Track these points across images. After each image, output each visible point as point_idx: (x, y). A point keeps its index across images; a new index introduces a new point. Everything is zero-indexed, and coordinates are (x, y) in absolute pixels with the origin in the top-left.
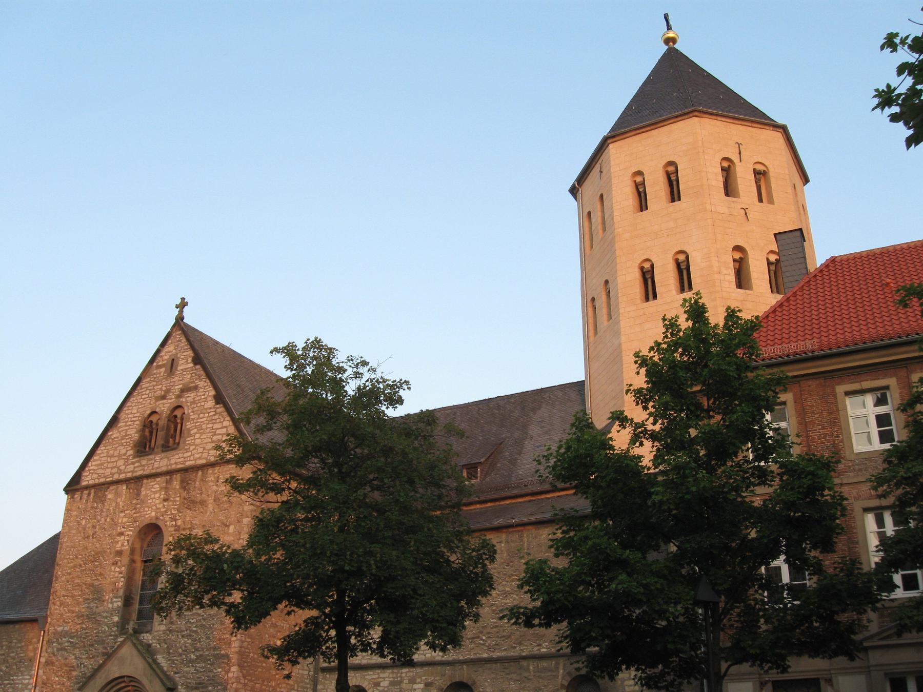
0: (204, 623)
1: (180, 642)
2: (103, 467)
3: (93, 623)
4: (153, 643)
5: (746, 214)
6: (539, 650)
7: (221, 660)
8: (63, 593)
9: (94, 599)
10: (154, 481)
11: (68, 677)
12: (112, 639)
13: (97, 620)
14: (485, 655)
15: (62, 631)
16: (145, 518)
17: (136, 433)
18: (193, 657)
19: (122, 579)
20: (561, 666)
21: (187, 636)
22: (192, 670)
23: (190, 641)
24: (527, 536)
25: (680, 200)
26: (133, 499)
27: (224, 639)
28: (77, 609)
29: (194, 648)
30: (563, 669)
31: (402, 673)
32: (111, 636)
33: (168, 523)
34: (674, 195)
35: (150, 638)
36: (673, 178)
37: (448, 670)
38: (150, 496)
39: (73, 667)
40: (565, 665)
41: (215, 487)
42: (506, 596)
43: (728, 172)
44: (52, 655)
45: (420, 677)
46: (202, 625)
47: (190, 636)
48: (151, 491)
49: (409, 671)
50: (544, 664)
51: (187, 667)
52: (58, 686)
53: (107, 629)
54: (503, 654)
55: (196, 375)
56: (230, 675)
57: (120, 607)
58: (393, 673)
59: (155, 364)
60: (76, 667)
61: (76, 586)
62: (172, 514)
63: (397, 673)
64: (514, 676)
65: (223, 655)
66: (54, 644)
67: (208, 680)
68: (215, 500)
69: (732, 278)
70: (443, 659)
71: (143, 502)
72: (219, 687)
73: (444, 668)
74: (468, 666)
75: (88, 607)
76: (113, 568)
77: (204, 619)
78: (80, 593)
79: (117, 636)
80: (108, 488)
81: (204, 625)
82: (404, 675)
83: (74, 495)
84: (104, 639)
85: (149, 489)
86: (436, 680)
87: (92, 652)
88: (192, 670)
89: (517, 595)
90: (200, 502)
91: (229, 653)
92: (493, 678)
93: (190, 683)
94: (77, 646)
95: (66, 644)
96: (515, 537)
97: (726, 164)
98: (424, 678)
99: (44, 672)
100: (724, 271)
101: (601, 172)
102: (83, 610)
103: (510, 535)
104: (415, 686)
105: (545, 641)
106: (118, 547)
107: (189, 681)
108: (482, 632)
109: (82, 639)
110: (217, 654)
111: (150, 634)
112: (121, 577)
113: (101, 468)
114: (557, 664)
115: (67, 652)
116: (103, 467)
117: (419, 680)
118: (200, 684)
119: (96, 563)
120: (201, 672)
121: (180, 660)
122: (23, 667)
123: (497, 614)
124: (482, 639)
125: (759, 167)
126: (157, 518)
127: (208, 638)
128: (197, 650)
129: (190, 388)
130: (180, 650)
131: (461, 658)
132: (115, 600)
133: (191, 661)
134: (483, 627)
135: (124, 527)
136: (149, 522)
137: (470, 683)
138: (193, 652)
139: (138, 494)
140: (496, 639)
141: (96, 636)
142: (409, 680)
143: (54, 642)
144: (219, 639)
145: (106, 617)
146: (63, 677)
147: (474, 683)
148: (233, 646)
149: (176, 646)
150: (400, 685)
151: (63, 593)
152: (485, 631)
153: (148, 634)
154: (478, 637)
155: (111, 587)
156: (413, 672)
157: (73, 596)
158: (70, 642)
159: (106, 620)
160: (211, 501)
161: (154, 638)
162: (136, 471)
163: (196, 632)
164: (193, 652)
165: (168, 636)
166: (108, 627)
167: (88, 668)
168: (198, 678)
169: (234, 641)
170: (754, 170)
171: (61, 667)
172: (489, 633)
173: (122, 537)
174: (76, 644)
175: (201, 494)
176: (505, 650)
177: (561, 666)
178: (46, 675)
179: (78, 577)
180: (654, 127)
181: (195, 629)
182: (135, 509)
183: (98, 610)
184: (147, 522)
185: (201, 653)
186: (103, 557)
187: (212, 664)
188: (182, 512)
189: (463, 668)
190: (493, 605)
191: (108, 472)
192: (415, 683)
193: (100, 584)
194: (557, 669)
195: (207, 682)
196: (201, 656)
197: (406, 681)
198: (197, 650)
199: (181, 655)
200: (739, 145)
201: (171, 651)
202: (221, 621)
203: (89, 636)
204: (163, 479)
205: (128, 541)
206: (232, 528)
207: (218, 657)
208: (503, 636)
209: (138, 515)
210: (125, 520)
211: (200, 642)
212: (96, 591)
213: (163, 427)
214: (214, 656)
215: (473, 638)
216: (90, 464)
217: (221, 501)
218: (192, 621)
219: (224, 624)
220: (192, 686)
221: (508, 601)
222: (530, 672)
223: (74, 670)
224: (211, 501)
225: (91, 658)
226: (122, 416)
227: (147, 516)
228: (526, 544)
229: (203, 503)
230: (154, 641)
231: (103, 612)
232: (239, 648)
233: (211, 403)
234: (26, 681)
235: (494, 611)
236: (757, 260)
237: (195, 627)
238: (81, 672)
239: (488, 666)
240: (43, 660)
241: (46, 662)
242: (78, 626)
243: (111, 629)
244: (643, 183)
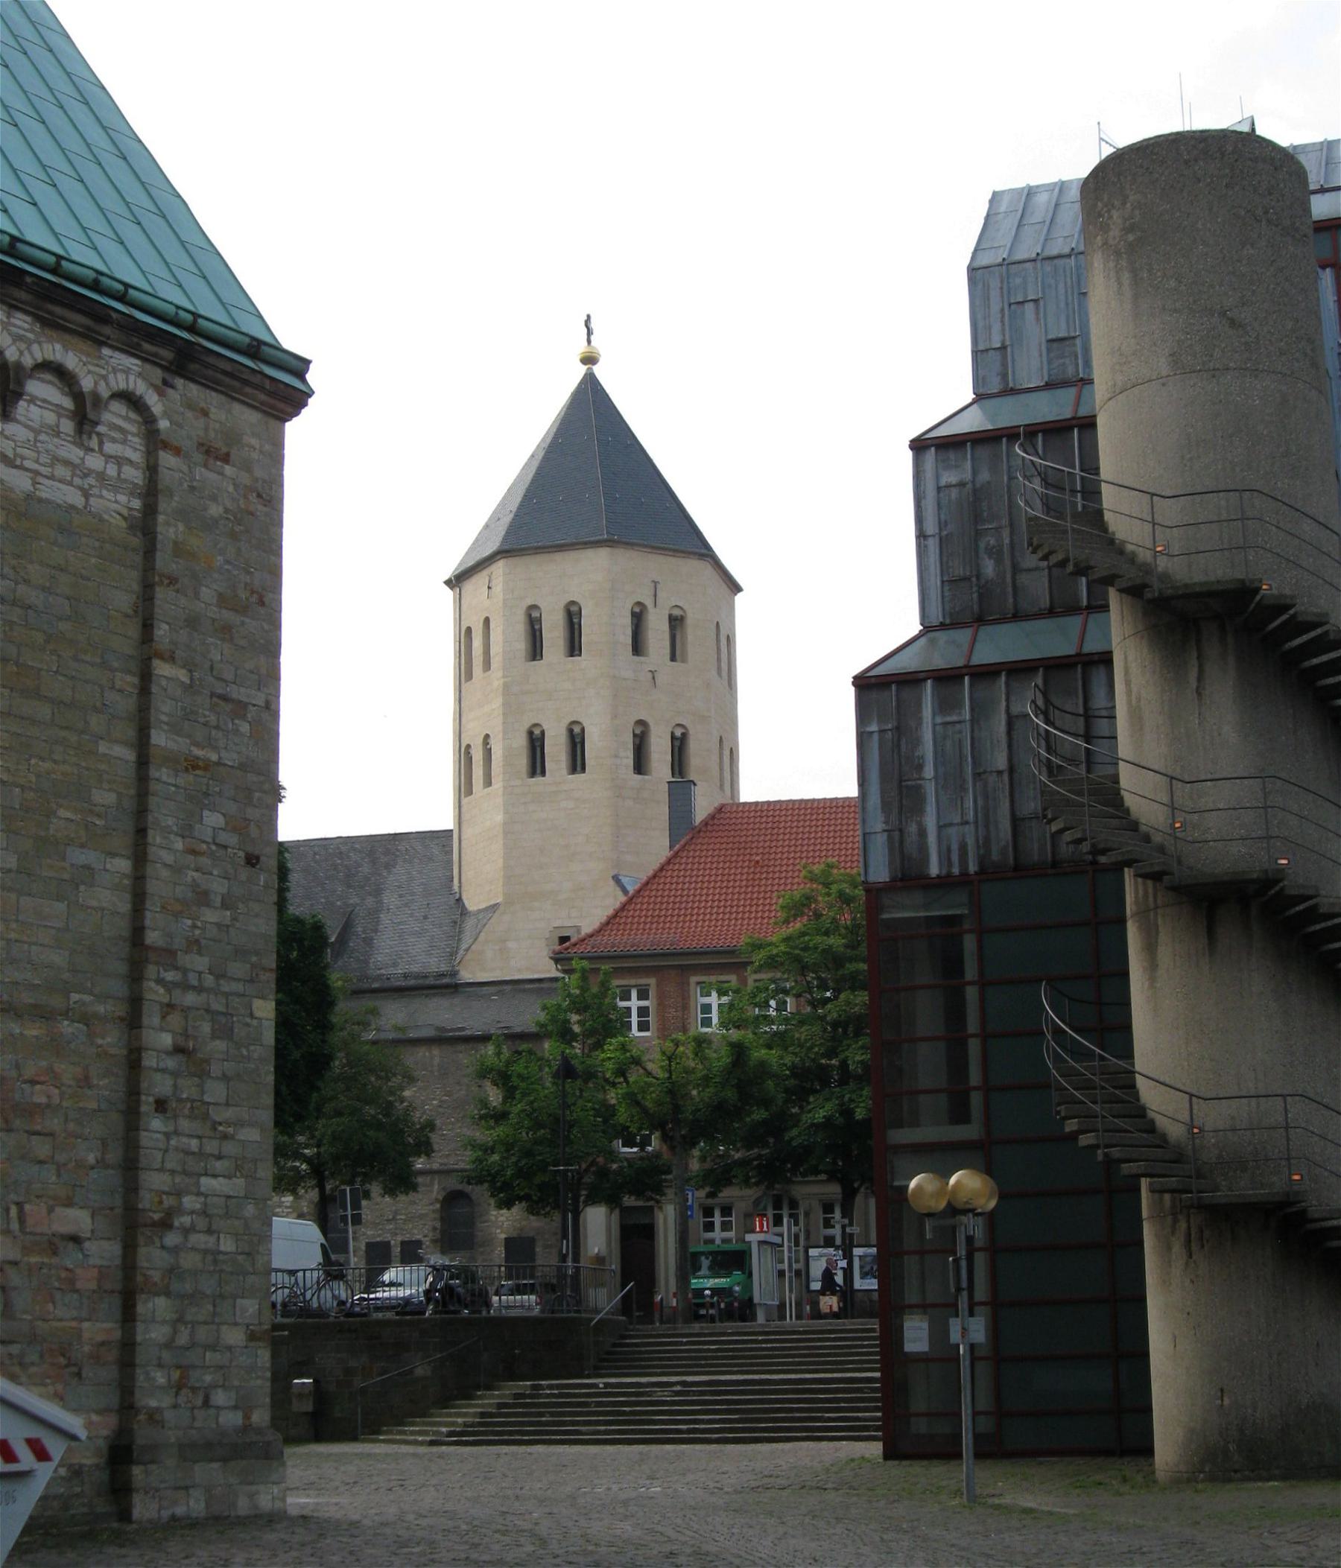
5: (654, 678)
20: (436, 1182)
25: (580, 655)
34: (574, 647)
36: (576, 621)
43: (638, 618)
69: (630, 762)
97: (637, 610)
100: (622, 754)
101: (489, 588)
125: (677, 612)
170: (670, 616)
177: (436, 1182)
200: (655, 583)
236: (660, 737)
244: (540, 620)
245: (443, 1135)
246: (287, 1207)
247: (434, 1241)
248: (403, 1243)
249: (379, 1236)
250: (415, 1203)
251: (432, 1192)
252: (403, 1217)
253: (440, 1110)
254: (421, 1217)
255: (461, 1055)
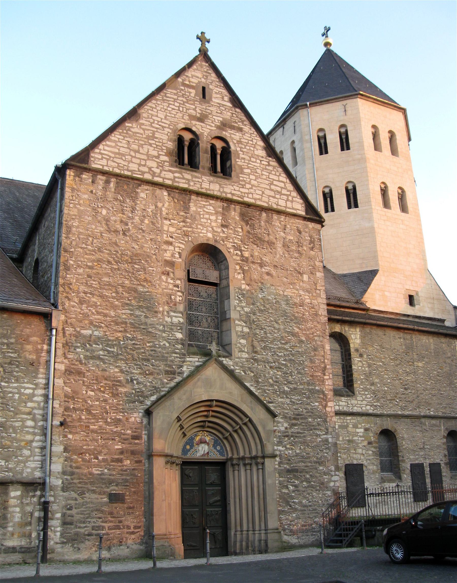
0: (293, 358)
1: (269, 373)
2: (124, 158)
3: (143, 335)
4: (236, 369)
6: (429, 412)
7: (316, 395)
8: (82, 288)
9: (141, 307)
10: (206, 202)
11: (112, 393)
12: (177, 357)
13: (150, 332)
14: (400, 413)
15: (91, 335)
16: (199, 236)
17: (169, 140)
18: (286, 389)
19: (179, 294)
21: (276, 368)
22: (288, 401)
23: (279, 373)
24: (415, 338)
26: (180, 210)
27: (317, 376)
28: (112, 313)
29: (287, 380)
30: (443, 426)
31: (347, 420)
32: (176, 353)
33: (232, 250)
35: (231, 363)
37: (378, 420)
38: (203, 215)
39: (119, 381)
40: (443, 423)
41: (282, 234)
42: (407, 375)
44: (77, 363)
45: (361, 424)
46: (291, 360)
47: (280, 368)
48: (204, 211)
49: (352, 419)
50: (433, 422)
51: (281, 398)
52: (97, 403)
53: (167, 345)
54: (410, 413)
55: (237, 117)
56: (328, 409)
57: (182, 323)
58: (340, 419)
59: (180, 80)
60: (124, 382)
61: (105, 285)
62: (234, 243)
63: (344, 419)
64: (417, 428)
65: (318, 391)
66: (78, 350)
67: (307, 412)
68: (284, 246)
70: (374, 412)
71: (194, 219)
72: (319, 420)
73: (376, 418)
74: (390, 418)
75: (131, 314)
76: (164, 278)
77: (293, 355)
78: (114, 294)
79: (184, 355)
80: (140, 185)
81: (294, 360)
82: (348, 421)
83: (82, 174)
84: (166, 355)
85: (200, 207)
86: (372, 427)
87: (148, 368)
88: (288, 401)
89: (413, 375)
90: (268, 242)
91: (324, 390)
92: (407, 429)
93: (287, 413)
94: (121, 357)
95: (101, 353)
96: (408, 337)
98: (363, 425)
99: (65, 383)
102: (124, 316)
103: (406, 335)
104: (358, 430)
105: (432, 408)
106: (167, 256)
107: (286, 411)
108: (396, 397)
109: (128, 350)
110: (312, 389)
111: (231, 359)
112: (178, 291)
113: (122, 159)
114: (440, 422)
115: (104, 363)
116: (124, 158)
117: (360, 426)
118: (298, 415)
119: (136, 266)
120: (297, 404)
121: (272, 390)
122: (17, 372)
123: (403, 385)
124: (397, 402)
126: (216, 241)
127: (299, 373)
128: (289, 382)
129: (234, 126)
130: (270, 381)
131: (385, 413)
132: (172, 314)
133: (284, 392)
134: (396, 393)
135: (172, 237)
136: (205, 242)
137: (393, 431)
138: (285, 384)
139: (186, 208)
140: (405, 402)
141: (152, 351)
142: (353, 425)
143: (78, 347)
144: (312, 376)
145: (164, 331)
146: (104, 392)
147: (396, 430)
148: (327, 383)
149: (265, 376)
150: (347, 428)
151: (82, 288)
152: (398, 396)
153: (227, 359)
154: (394, 400)
155: (165, 299)
156: (354, 419)
157: (101, 296)
158: (109, 352)
159: (164, 335)
160: (280, 245)
161: (236, 364)
162: (178, 182)
163: (285, 365)
164: (285, 384)
165: (253, 364)
166: (169, 343)
167: (145, 386)
168: (295, 409)
169: (327, 379)
171: (96, 380)
172: (400, 398)
173: (171, 248)
174: (118, 354)
175: (268, 235)
176: (411, 410)
178: (70, 387)
179: (108, 275)
180: (383, 104)
181: (284, 363)
182: (184, 221)
183: (149, 321)
184: (201, 241)
185: (295, 386)
186: (146, 261)
187: (308, 398)
188: (248, 245)
189: (387, 420)
190: (400, 379)
191: (134, 167)
192: (357, 428)
193: (147, 292)
194: (440, 426)
195: (306, 414)
196: (295, 389)
197: (351, 426)
198: (289, 382)
199: (272, 385)
201: (260, 380)
202: (310, 359)
203: (139, 349)
204: (219, 204)
205: (179, 253)
206: (305, 277)
207: (313, 392)
208: (409, 401)
209: (189, 229)
210: (172, 229)
211: (292, 376)
212: (141, 297)
213: (206, 150)
214: (310, 390)
215: (391, 400)
216: (101, 147)
217: (290, 249)
218: (280, 354)
219: (314, 363)
220: (290, 417)
221: (409, 378)
222: (426, 426)
223: (123, 386)
224: (279, 245)
225: (147, 374)
226: (143, 112)
227: (201, 235)
228: (415, 343)
229: (271, 244)
230: (237, 368)
231: (157, 324)
232: (332, 387)
233: (263, 153)
234: (28, 391)
235: (401, 383)
237: (284, 360)
238: (134, 389)
239: (402, 419)
240: (62, 367)
241: (66, 370)
242: (119, 334)
243: (174, 346)
245: (441, 394)
246: (360, 436)
247: (446, 464)
248: (430, 465)
249: (417, 459)
250: (434, 438)
251: (440, 430)
252: (428, 447)
253: (438, 378)
254: (438, 446)
255: (444, 345)
